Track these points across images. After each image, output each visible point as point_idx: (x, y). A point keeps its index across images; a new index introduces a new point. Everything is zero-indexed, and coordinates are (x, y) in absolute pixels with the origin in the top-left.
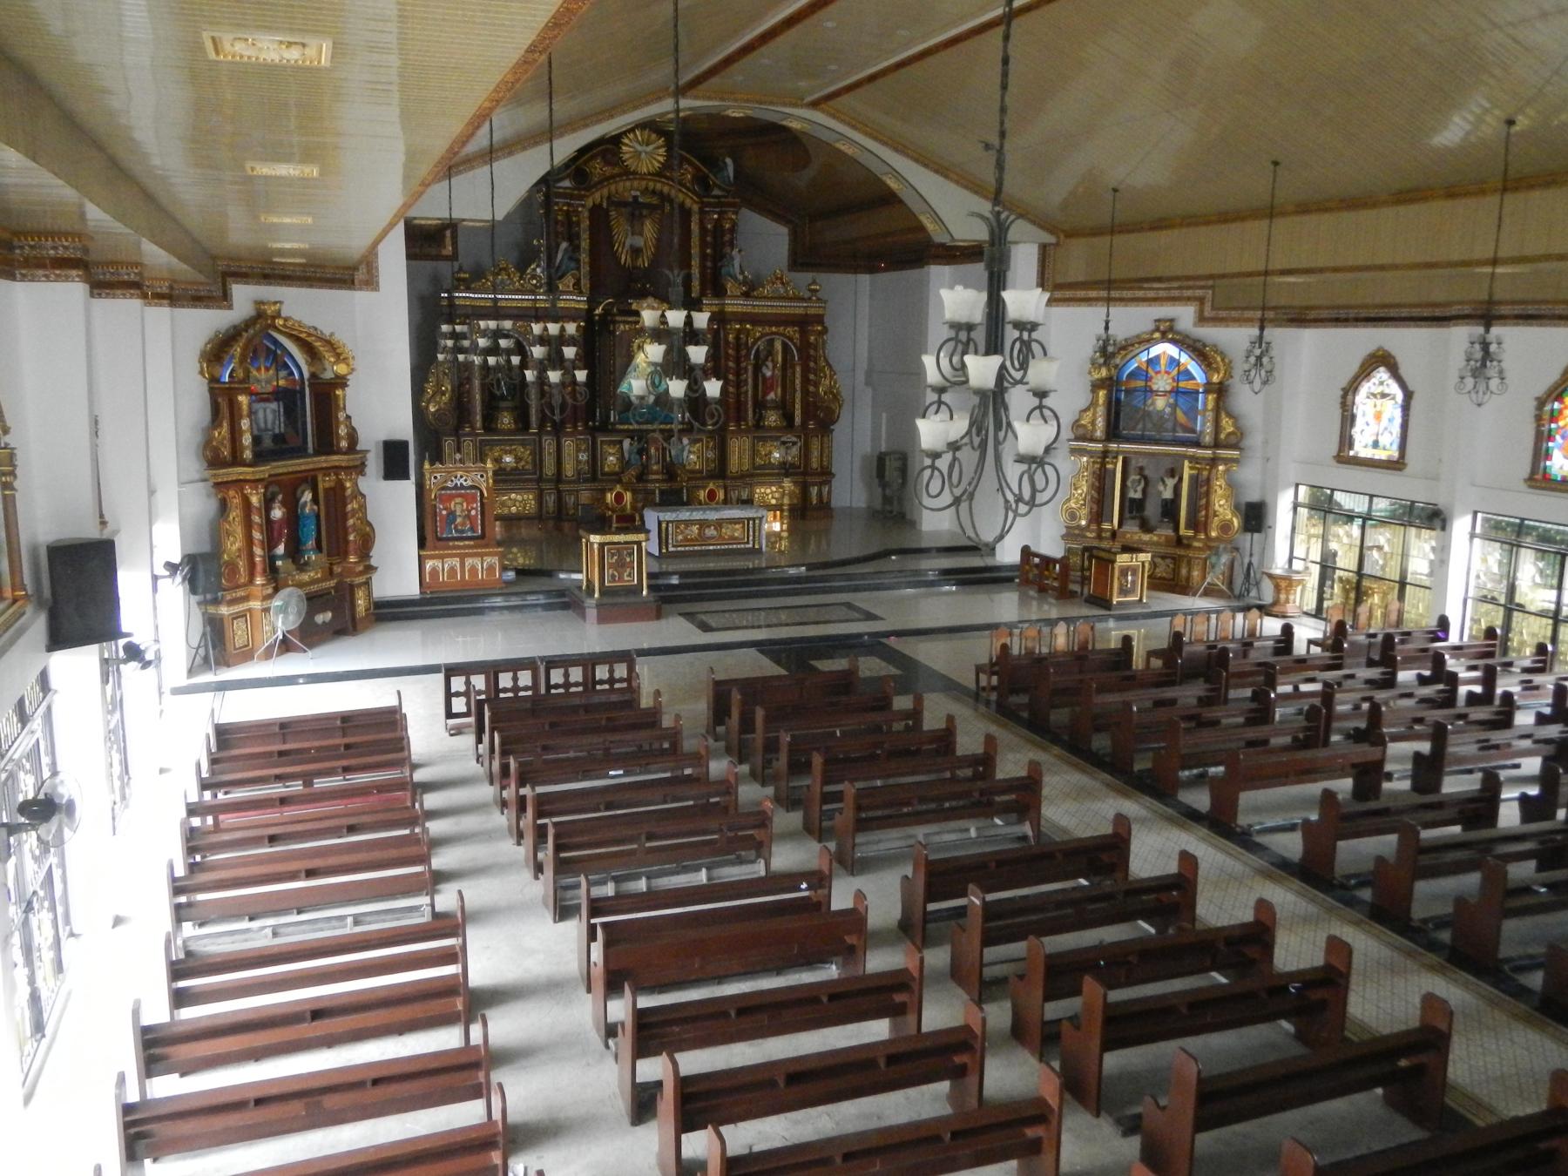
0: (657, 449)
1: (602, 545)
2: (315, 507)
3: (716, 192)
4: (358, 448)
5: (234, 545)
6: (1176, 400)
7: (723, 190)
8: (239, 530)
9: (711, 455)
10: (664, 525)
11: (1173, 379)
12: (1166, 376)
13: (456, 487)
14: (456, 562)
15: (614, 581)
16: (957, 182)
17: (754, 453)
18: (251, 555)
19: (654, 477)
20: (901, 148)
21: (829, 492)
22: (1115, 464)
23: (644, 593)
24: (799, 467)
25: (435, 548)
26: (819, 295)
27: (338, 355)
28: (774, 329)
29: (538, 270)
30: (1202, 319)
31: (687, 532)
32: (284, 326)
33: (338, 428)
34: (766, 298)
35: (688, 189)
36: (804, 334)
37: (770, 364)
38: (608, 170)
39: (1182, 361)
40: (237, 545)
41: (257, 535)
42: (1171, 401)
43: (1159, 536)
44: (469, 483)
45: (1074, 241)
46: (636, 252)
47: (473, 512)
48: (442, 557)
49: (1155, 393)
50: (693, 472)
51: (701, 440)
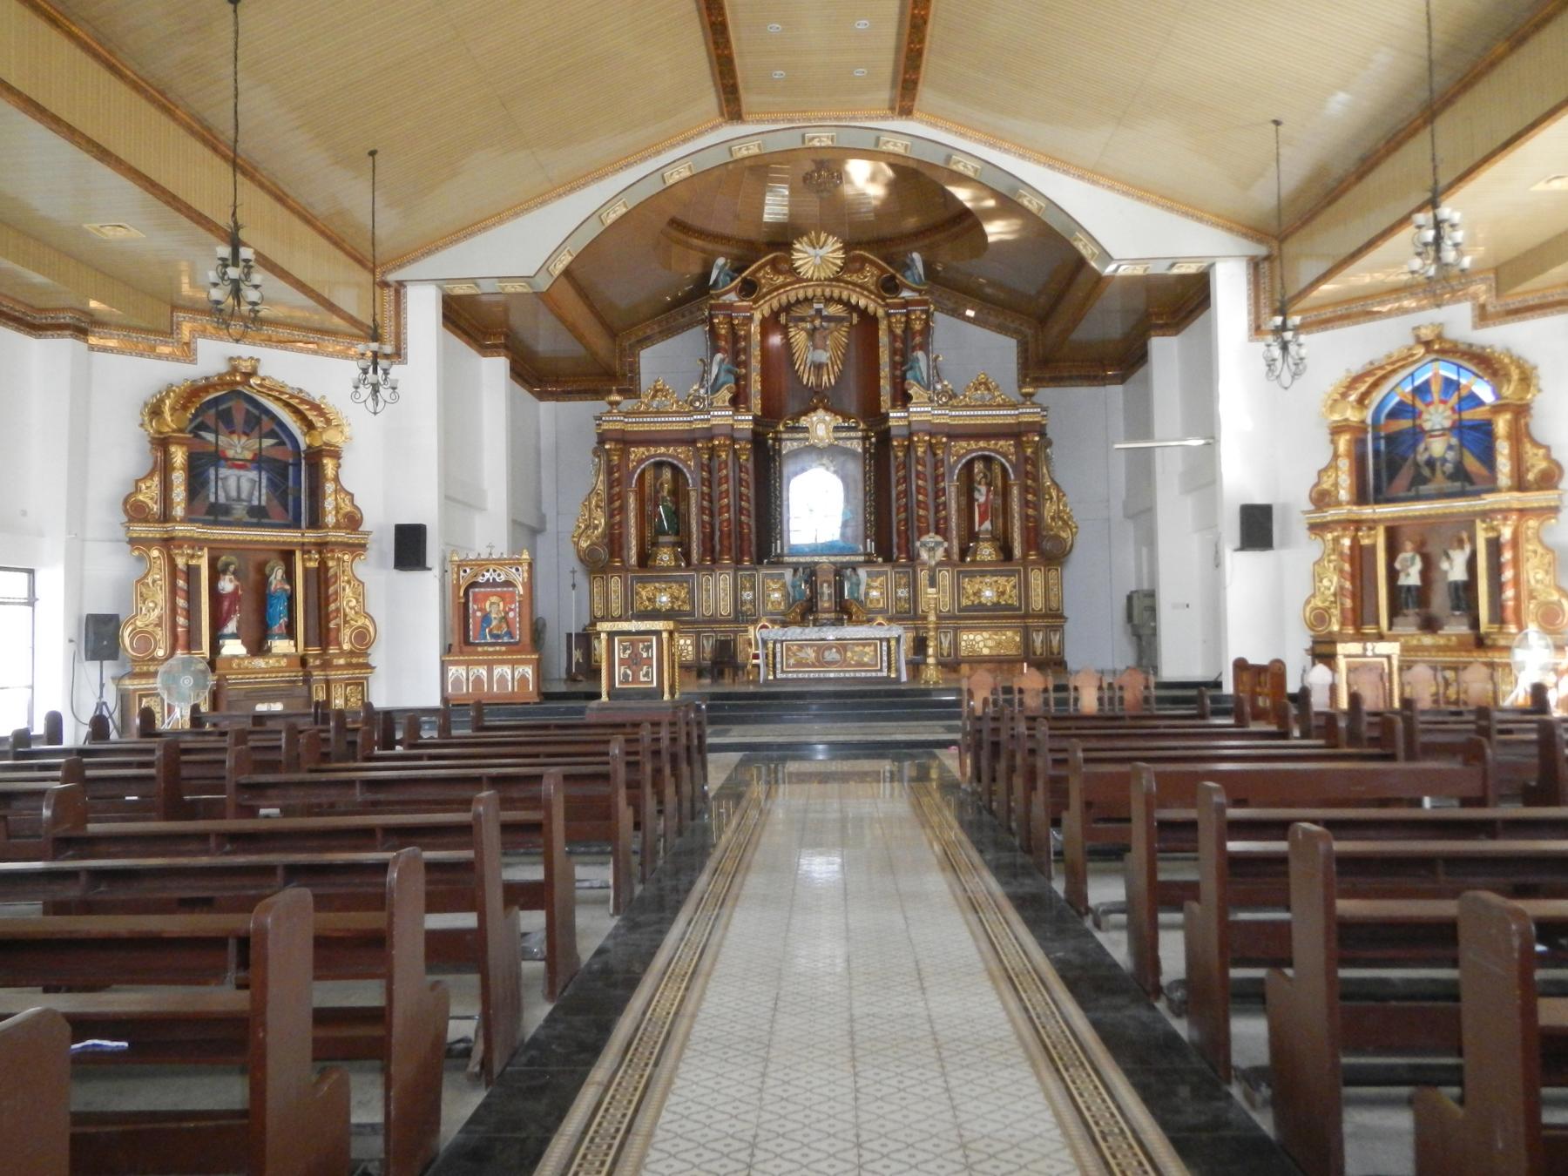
0: (829, 583)
1: (611, 635)
2: (287, 587)
3: (906, 294)
4: (364, 527)
5: (154, 610)
6: (1461, 439)
7: (913, 290)
8: (161, 597)
9: (903, 593)
10: (770, 645)
11: (1453, 409)
12: (1441, 407)
13: (487, 584)
14: (483, 671)
15: (627, 682)
16: (1111, 188)
17: (958, 589)
18: (174, 625)
20: (1025, 151)
21: (1061, 642)
22: (1376, 536)
23: (666, 697)
24: (1019, 609)
25: (461, 653)
26: (1035, 399)
27: (328, 422)
28: (982, 444)
29: (702, 391)
30: (1483, 317)
31: (801, 655)
32: (261, 385)
33: (324, 499)
34: (967, 406)
35: (870, 292)
36: (1019, 446)
37: (983, 489)
38: (780, 280)
39: (1463, 381)
40: (157, 612)
41: (181, 602)
42: (1454, 441)
43: (1448, 637)
44: (503, 578)
45: (1291, 247)
46: (818, 367)
47: (511, 614)
48: (468, 664)
49: (1430, 434)
51: (886, 573)
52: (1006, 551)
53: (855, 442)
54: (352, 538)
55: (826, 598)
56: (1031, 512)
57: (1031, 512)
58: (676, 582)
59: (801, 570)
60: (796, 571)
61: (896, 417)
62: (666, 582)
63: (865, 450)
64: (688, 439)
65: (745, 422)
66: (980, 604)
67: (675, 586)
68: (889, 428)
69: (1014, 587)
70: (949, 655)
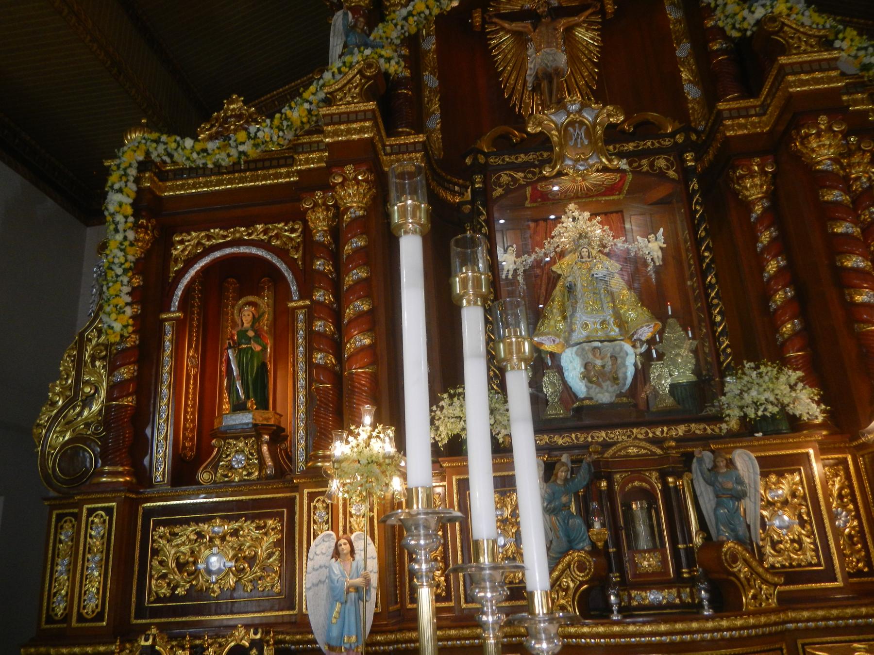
19: (653, 596)
50: (792, 575)
53: (661, 163)
55: (644, 542)
58: (252, 518)
62: (229, 519)
63: (686, 174)
67: (249, 529)
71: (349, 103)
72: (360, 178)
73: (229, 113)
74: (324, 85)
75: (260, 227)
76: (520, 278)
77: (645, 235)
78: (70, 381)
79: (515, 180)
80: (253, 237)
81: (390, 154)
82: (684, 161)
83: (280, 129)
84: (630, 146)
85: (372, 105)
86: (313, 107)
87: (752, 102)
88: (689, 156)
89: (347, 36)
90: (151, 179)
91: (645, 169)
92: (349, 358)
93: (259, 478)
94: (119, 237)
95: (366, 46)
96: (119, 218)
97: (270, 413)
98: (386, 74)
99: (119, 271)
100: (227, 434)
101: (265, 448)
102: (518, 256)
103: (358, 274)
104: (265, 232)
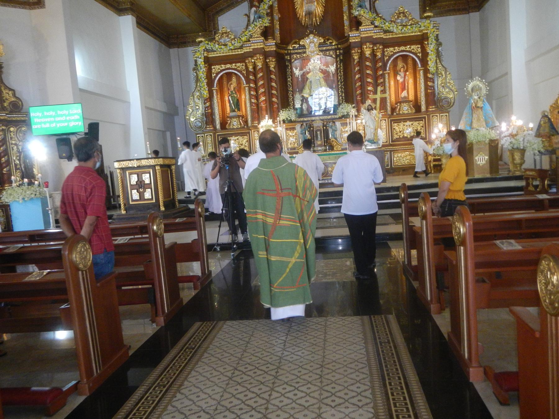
28: (403, 48)
46: (309, 14)
52: (417, 108)
53: (331, 53)
54: (15, 117)
55: (319, 139)
56: (430, 84)
57: (430, 84)
58: (241, 136)
59: (304, 124)
60: (302, 125)
61: (354, 36)
64: (242, 58)
65: (271, 45)
66: (404, 137)
67: (240, 138)
68: (350, 42)
69: (423, 126)
70: (388, 166)
71: (257, 37)
72: (261, 58)
73: (223, 32)
74: (250, 31)
75: (234, 64)
76: (300, 77)
77: (331, 65)
78: (192, 105)
79: (297, 57)
80: (233, 67)
81: (267, 46)
82: (336, 53)
83: (240, 43)
84: (324, 48)
85: (263, 38)
86: (248, 37)
87: (358, 32)
88: (338, 51)
89: (255, 15)
90: (207, 54)
91: (328, 54)
92: (261, 102)
93: (240, 128)
94: (202, 70)
95: (260, 17)
96: (201, 65)
97: (241, 112)
98: (265, 27)
99: (203, 79)
100: (231, 118)
101: (241, 120)
102: (299, 71)
103: (261, 83)
104: (236, 66)
